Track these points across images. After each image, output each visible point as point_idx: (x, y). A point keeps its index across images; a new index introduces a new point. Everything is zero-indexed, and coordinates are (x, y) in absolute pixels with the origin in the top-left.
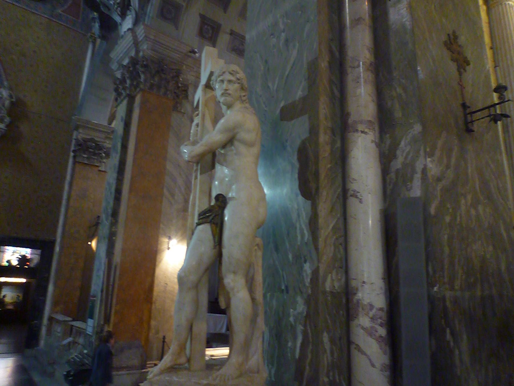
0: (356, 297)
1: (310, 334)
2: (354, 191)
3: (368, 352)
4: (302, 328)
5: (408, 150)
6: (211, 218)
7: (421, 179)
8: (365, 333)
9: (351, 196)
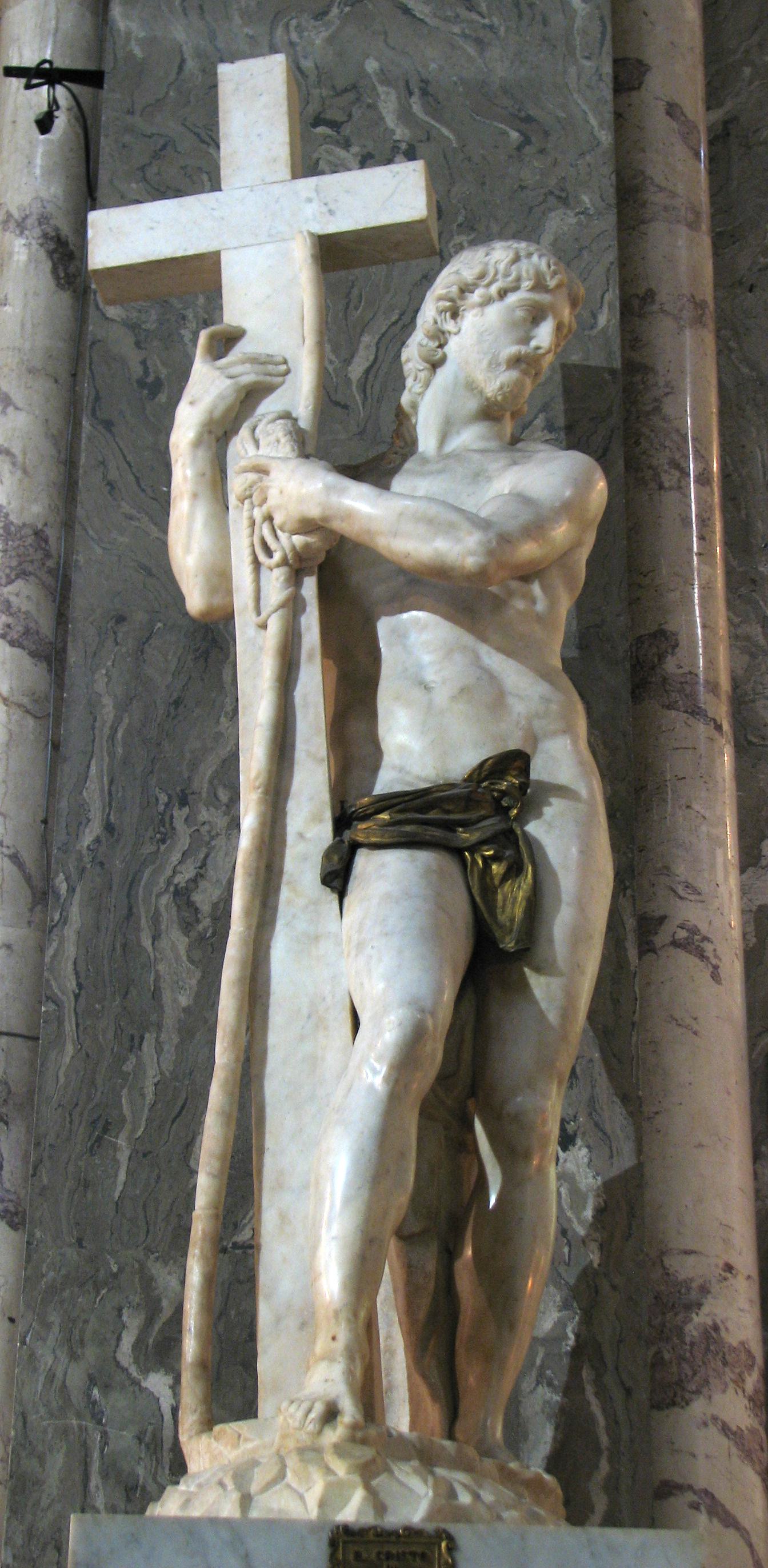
0: (700, 1319)
1: (601, 1421)
2: (694, 931)
3: (746, 1522)
4: (557, 1398)
6: (466, 836)
8: (734, 1450)
9: (675, 944)
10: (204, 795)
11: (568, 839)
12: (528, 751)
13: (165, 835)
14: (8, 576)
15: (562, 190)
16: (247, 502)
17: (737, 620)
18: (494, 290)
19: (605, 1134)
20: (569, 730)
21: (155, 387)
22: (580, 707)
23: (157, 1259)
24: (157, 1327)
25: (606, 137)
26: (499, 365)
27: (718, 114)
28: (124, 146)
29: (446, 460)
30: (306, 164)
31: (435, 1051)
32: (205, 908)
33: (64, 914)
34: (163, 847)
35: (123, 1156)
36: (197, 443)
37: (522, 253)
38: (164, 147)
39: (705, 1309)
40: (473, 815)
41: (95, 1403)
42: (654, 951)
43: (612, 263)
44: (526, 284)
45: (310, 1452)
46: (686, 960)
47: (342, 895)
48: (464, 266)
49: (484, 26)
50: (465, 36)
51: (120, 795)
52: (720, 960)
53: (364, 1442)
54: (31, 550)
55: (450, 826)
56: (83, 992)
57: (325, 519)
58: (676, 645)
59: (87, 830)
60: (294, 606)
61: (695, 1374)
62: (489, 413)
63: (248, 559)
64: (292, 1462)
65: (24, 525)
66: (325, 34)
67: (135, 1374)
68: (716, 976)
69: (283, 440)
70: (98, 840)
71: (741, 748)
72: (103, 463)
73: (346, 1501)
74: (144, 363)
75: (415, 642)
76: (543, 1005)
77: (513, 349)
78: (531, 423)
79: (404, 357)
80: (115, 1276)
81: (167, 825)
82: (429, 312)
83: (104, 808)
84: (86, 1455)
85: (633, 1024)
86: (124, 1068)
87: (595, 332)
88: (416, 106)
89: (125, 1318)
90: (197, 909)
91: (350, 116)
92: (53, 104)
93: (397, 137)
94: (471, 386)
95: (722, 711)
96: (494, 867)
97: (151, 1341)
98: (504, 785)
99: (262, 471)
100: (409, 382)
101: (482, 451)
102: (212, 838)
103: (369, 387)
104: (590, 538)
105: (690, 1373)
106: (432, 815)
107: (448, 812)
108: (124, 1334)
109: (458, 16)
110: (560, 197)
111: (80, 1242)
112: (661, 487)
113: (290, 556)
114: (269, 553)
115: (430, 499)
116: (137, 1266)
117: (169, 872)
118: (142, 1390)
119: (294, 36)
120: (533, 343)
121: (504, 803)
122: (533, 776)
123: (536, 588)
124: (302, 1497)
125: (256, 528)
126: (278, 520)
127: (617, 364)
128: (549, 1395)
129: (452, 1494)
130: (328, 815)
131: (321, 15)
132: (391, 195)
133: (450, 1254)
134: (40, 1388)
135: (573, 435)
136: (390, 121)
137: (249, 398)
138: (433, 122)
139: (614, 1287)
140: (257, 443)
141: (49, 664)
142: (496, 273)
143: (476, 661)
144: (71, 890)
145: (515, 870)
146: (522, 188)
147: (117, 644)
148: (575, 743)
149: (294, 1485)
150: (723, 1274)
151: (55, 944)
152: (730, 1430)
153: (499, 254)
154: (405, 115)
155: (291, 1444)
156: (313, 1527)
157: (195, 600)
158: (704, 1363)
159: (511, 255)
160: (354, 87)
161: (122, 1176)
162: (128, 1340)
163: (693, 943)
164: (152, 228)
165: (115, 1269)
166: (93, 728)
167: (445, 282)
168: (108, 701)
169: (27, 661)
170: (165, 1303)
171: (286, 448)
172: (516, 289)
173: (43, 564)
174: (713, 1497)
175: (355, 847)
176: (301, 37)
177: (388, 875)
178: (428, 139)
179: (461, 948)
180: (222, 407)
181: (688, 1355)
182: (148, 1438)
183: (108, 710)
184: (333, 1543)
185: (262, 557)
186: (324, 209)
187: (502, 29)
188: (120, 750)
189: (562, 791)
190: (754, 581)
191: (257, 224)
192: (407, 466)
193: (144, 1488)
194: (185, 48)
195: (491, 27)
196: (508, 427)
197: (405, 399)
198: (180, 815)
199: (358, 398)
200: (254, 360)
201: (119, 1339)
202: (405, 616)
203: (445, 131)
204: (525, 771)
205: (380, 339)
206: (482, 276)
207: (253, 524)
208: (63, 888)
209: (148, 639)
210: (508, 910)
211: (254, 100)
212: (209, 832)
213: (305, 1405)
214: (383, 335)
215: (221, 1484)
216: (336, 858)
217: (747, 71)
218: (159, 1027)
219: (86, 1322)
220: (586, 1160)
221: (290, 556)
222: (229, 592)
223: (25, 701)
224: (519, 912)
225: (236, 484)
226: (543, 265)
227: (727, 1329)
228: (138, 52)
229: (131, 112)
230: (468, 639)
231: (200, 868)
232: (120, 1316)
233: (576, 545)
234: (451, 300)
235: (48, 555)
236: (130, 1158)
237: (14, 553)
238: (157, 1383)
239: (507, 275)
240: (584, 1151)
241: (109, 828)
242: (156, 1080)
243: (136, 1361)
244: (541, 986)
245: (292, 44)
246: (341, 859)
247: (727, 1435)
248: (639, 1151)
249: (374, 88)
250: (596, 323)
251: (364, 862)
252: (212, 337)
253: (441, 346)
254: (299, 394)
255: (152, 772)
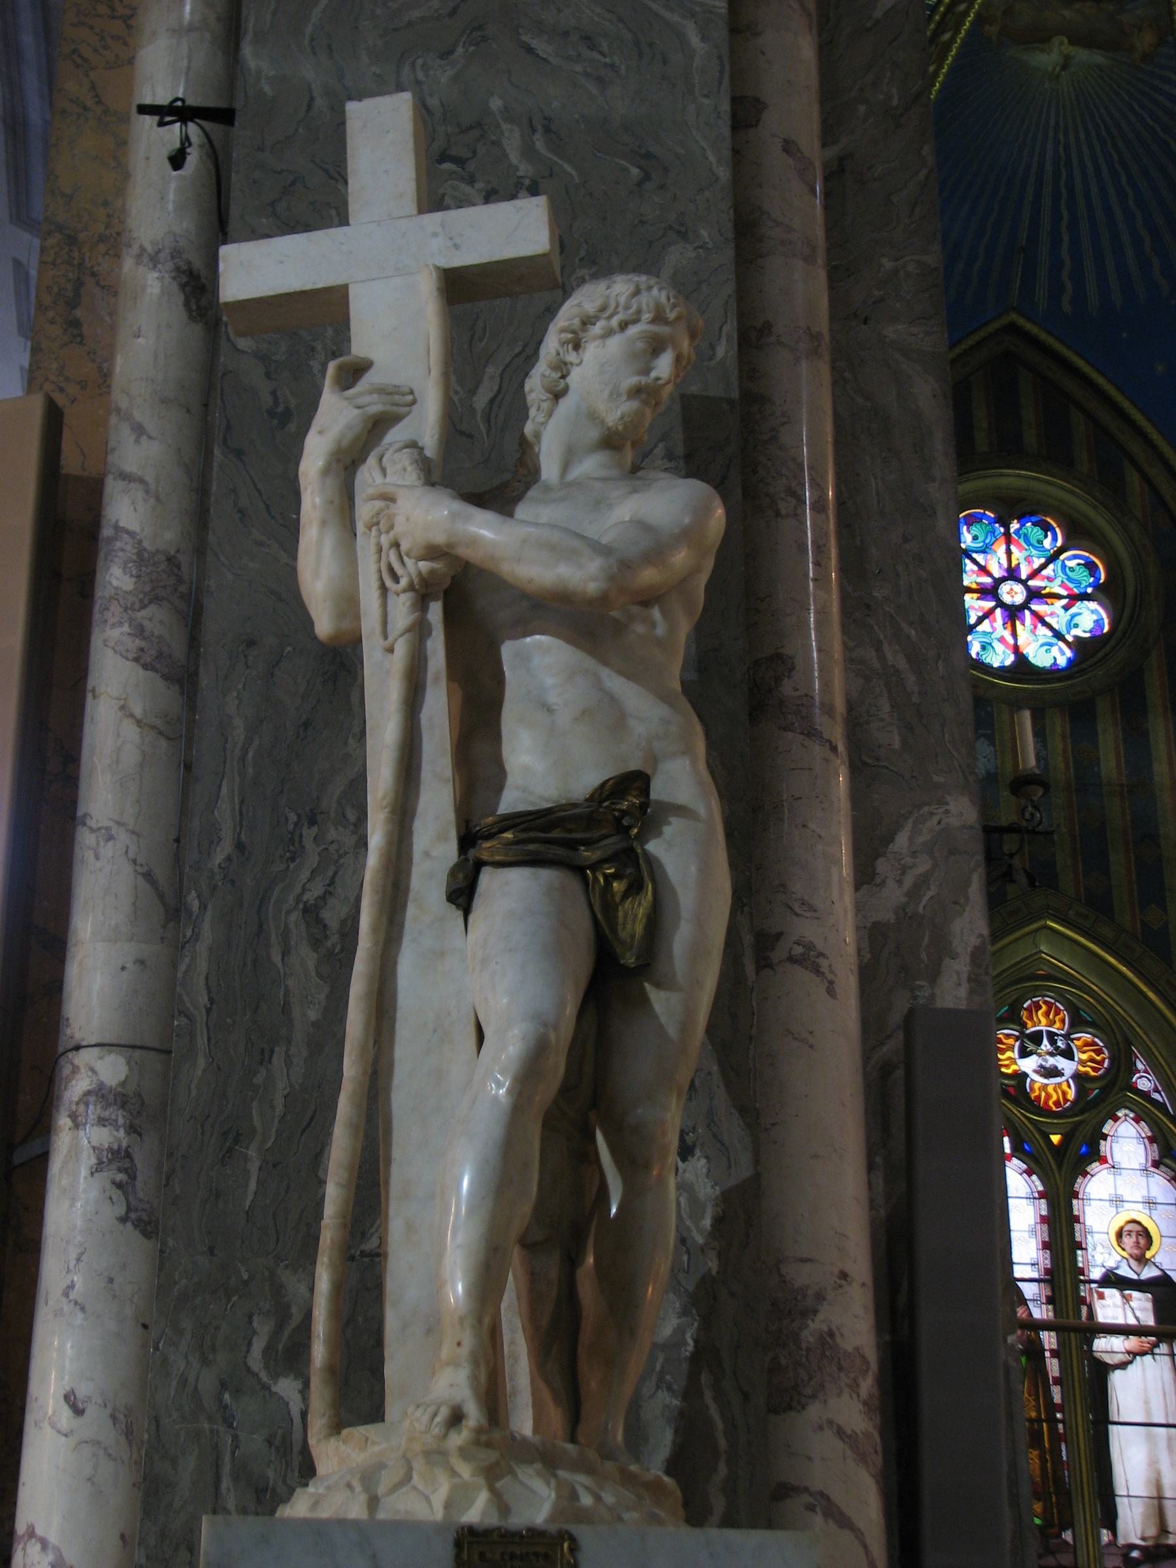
0: (816, 1325)
2: (810, 947)
4: (676, 1402)
5: (920, 870)
6: (587, 855)
7: (969, 980)
8: (849, 1453)
9: (791, 959)
10: (333, 814)
11: (687, 858)
12: (649, 772)
13: (295, 854)
14: (141, 601)
15: (682, 225)
16: (374, 529)
17: (851, 644)
18: (615, 322)
19: (723, 1145)
20: (688, 751)
21: (285, 417)
22: (699, 729)
23: (287, 1267)
24: (286, 1333)
25: (723, 173)
26: (620, 395)
27: (833, 151)
28: (255, 182)
29: (569, 487)
30: (432, 199)
31: (557, 1066)
32: (334, 924)
33: (196, 930)
34: (292, 866)
35: (254, 1167)
36: (326, 472)
37: (643, 286)
38: (293, 183)
39: (821, 1316)
40: (594, 834)
41: (226, 1407)
42: (771, 966)
43: (730, 296)
44: (647, 316)
45: (436, 1456)
46: (802, 975)
47: (467, 912)
48: (586, 299)
49: (605, 65)
50: (587, 75)
51: (251, 814)
52: (836, 975)
53: (489, 1445)
54: (164, 576)
55: (572, 845)
56: (214, 1007)
57: (451, 545)
58: (792, 669)
59: (219, 849)
60: (420, 630)
61: (811, 1378)
62: (610, 442)
63: (375, 584)
64: (418, 1465)
65: (157, 551)
66: (450, 73)
67: (265, 1379)
68: (831, 991)
69: (409, 469)
70: (229, 859)
71: (856, 769)
72: (234, 491)
73: (472, 1502)
74: (274, 393)
75: (538, 664)
76: (663, 1020)
77: (634, 380)
78: (651, 451)
79: (527, 388)
80: (246, 1283)
81: (297, 845)
82: (551, 344)
83: (235, 827)
84: (218, 1458)
85: (751, 1038)
86: (255, 1081)
87: (714, 362)
88: (539, 143)
89: (255, 1324)
90: (325, 926)
91: (475, 152)
92: (186, 141)
93: (520, 173)
94: (593, 416)
95: (837, 733)
96: (615, 885)
97: (280, 1347)
98: (625, 805)
99: (389, 499)
100: (532, 412)
101: (604, 480)
102: (341, 857)
103: (493, 416)
104: (709, 564)
105: (806, 1378)
106: (555, 834)
107: (570, 831)
108: (255, 1340)
109: (580, 55)
110: (679, 232)
111: (211, 1250)
112: (778, 514)
113: (416, 581)
114: (396, 578)
115: (553, 526)
116: (267, 1274)
117: (298, 890)
118: (272, 1394)
119: (420, 75)
120: (653, 374)
121: (625, 822)
122: (654, 796)
123: (656, 613)
124: (427, 1499)
125: (383, 554)
126: (404, 547)
127: (735, 395)
128: (668, 1399)
129: (574, 1496)
130: (453, 834)
131: (446, 54)
132: (517, 229)
133: (572, 1262)
134: (173, 1392)
135: (692, 465)
136: (514, 157)
137: (376, 427)
138: (555, 159)
139: (732, 1295)
140: (384, 471)
141: (182, 687)
142: (617, 306)
143: (598, 684)
144: (203, 907)
145: (635, 888)
146: (643, 223)
147: (248, 667)
148: (694, 764)
149: (421, 1487)
150: (839, 1281)
151: (187, 960)
152: (844, 1433)
153: (620, 287)
154: (528, 151)
155: (417, 1447)
156: (439, 1528)
157: (324, 625)
158: (820, 1368)
159: (632, 288)
160: (479, 124)
161: (253, 1186)
162: (258, 1346)
163: (809, 959)
164: (282, 262)
165: (246, 1277)
166: (224, 749)
167: (567, 314)
168: (238, 723)
169: (160, 684)
170: (294, 1310)
171: (412, 476)
172: (636, 321)
173: (176, 590)
174: (828, 1499)
175: (479, 865)
176: (427, 76)
177: (510, 891)
178: (551, 175)
179: (582, 962)
180: (350, 436)
181: (804, 1360)
182: (277, 1442)
183: (239, 731)
184: (458, 1544)
185: (389, 583)
186: (450, 243)
187: (623, 68)
188: (250, 771)
189: (681, 810)
190: (868, 606)
191: (384, 257)
192: (531, 493)
193: (274, 1490)
194: (314, 86)
195: (612, 66)
196: (629, 456)
197: (528, 429)
198: (309, 833)
199: (482, 427)
200: (382, 391)
201: (250, 1344)
202: (528, 639)
203: (568, 168)
204: (645, 791)
205: (504, 370)
206: (603, 309)
207: (380, 550)
208: (195, 905)
209: (278, 662)
210: (629, 926)
211: (381, 137)
212: (337, 851)
213: (431, 1410)
214: (507, 366)
215: (349, 1486)
216: (461, 876)
217: (862, 109)
218: (289, 1041)
219: (217, 1328)
220: (705, 1170)
221: (416, 581)
222: (357, 617)
223: (158, 723)
224: (639, 929)
225: (364, 511)
226: (663, 298)
227: (842, 1335)
228: (268, 90)
229: (261, 149)
230: (589, 662)
231: (329, 885)
232: (250, 1322)
233: (695, 570)
234: (574, 332)
235: (180, 581)
236: (260, 1169)
237: (147, 579)
238: (287, 1387)
239: (627, 308)
240: (703, 1161)
241: (240, 846)
242: (285, 1092)
243: (267, 1366)
244: (660, 1001)
245: (418, 82)
246: (465, 877)
247: (841, 1438)
248: (757, 1162)
249: (498, 126)
250: (714, 354)
251: (489, 880)
252: (340, 368)
253: (563, 377)
254: (425, 423)
255: (281, 792)
